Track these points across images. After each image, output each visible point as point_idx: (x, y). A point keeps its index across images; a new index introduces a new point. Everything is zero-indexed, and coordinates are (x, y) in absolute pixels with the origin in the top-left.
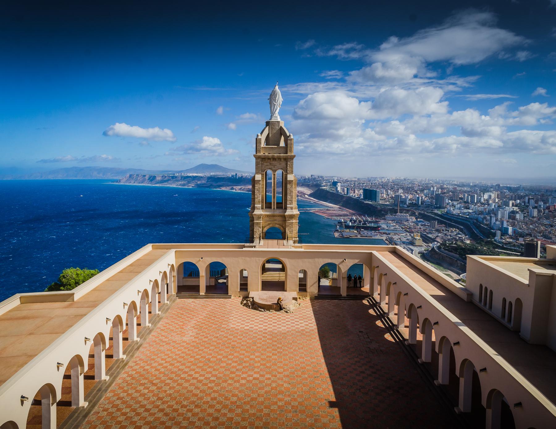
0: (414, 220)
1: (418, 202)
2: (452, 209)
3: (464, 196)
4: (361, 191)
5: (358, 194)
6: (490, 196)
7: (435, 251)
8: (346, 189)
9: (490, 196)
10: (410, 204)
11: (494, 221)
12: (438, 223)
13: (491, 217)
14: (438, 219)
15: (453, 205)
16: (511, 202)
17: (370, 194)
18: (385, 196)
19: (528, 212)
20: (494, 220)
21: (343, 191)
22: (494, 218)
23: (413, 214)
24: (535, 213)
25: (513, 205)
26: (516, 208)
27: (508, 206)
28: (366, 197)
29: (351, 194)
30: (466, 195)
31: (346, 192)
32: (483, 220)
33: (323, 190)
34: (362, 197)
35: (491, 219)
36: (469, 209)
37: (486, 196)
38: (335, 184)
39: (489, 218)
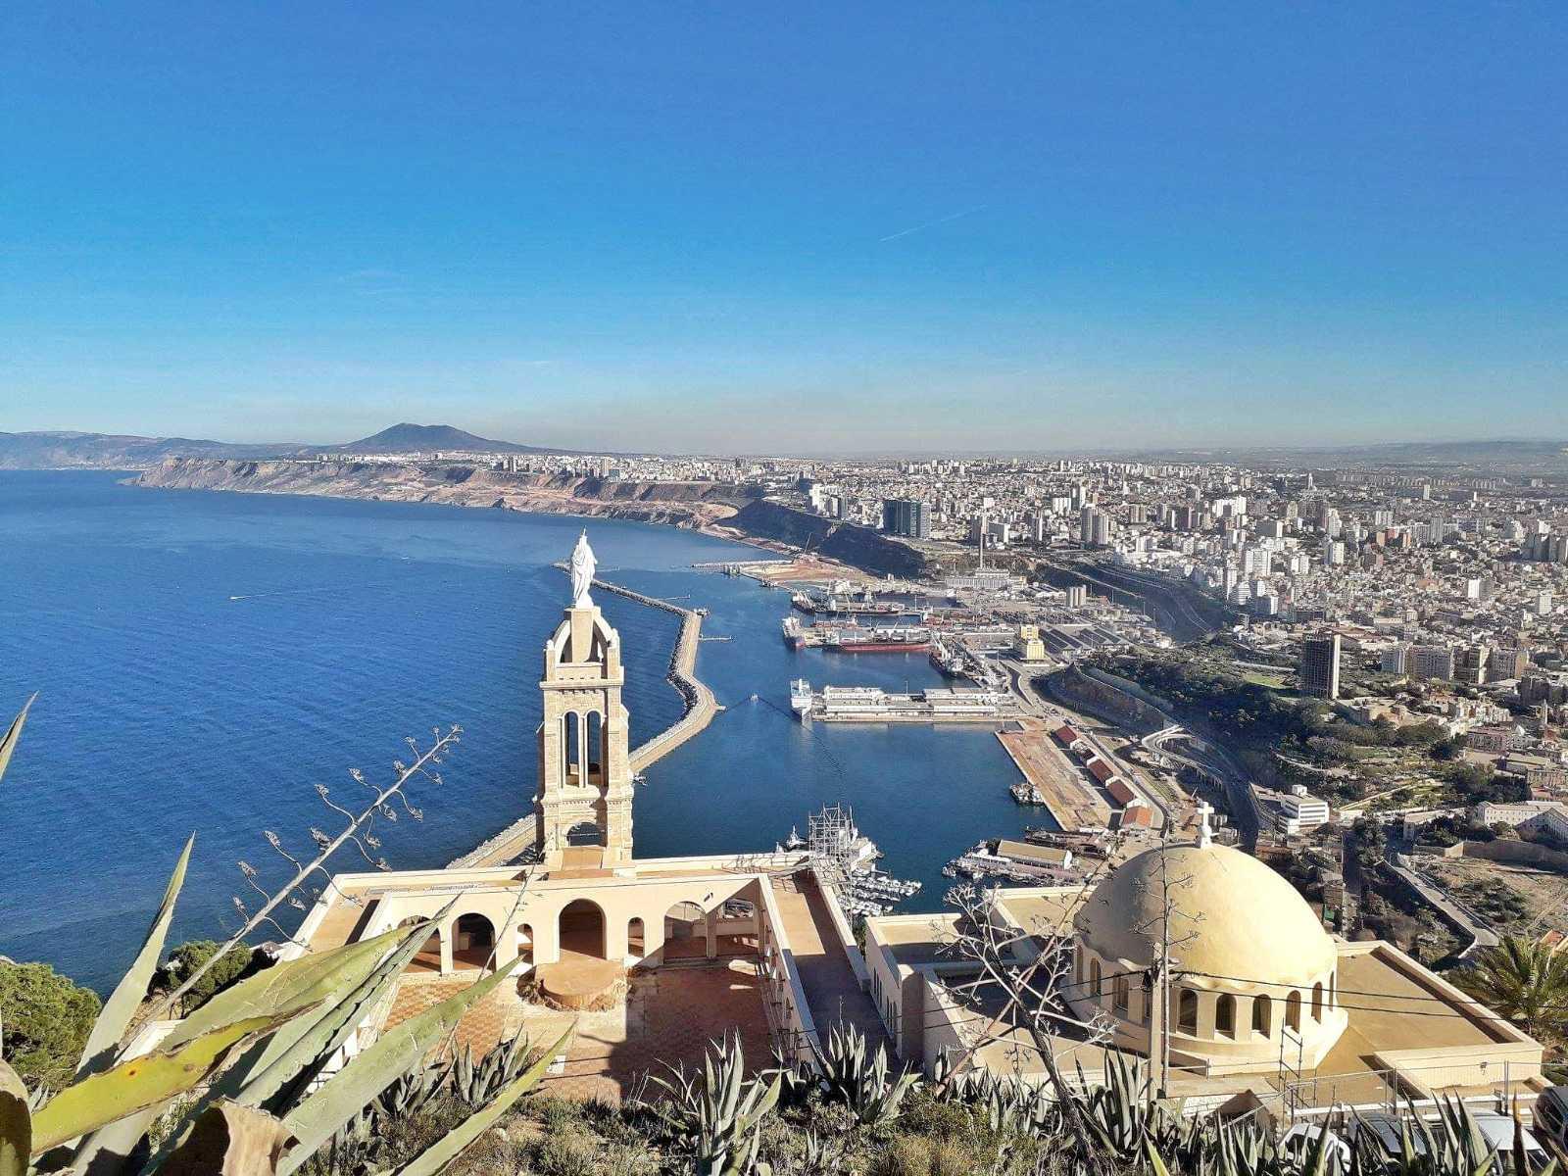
0: (1025, 586)
1: (1036, 534)
3: (1160, 509)
4: (880, 505)
5: (868, 514)
6: (1227, 509)
8: (835, 502)
9: (1227, 509)
10: (1015, 540)
12: (1088, 591)
13: (1225, 571)
14: (1087, 583)
16: (1280, 525)
18: (944, 518)
19: (1322, 552)
20: (1232, 577)
21: (829, 504)
22: (1235, 574)
23: (1021, 570)
24: (1339, 551)
25: (1285, 534)
26: (1293, 542)
27: (1273, 535)
28: (890, 527)
29: (851, 516)
30: (1165, 509)
31: (835, 509)
33: (771, 505)
34: (880, 525)
36: (1171, 548)
37: (1218, 508)
38: (804, 485)
39: (1220, 572)
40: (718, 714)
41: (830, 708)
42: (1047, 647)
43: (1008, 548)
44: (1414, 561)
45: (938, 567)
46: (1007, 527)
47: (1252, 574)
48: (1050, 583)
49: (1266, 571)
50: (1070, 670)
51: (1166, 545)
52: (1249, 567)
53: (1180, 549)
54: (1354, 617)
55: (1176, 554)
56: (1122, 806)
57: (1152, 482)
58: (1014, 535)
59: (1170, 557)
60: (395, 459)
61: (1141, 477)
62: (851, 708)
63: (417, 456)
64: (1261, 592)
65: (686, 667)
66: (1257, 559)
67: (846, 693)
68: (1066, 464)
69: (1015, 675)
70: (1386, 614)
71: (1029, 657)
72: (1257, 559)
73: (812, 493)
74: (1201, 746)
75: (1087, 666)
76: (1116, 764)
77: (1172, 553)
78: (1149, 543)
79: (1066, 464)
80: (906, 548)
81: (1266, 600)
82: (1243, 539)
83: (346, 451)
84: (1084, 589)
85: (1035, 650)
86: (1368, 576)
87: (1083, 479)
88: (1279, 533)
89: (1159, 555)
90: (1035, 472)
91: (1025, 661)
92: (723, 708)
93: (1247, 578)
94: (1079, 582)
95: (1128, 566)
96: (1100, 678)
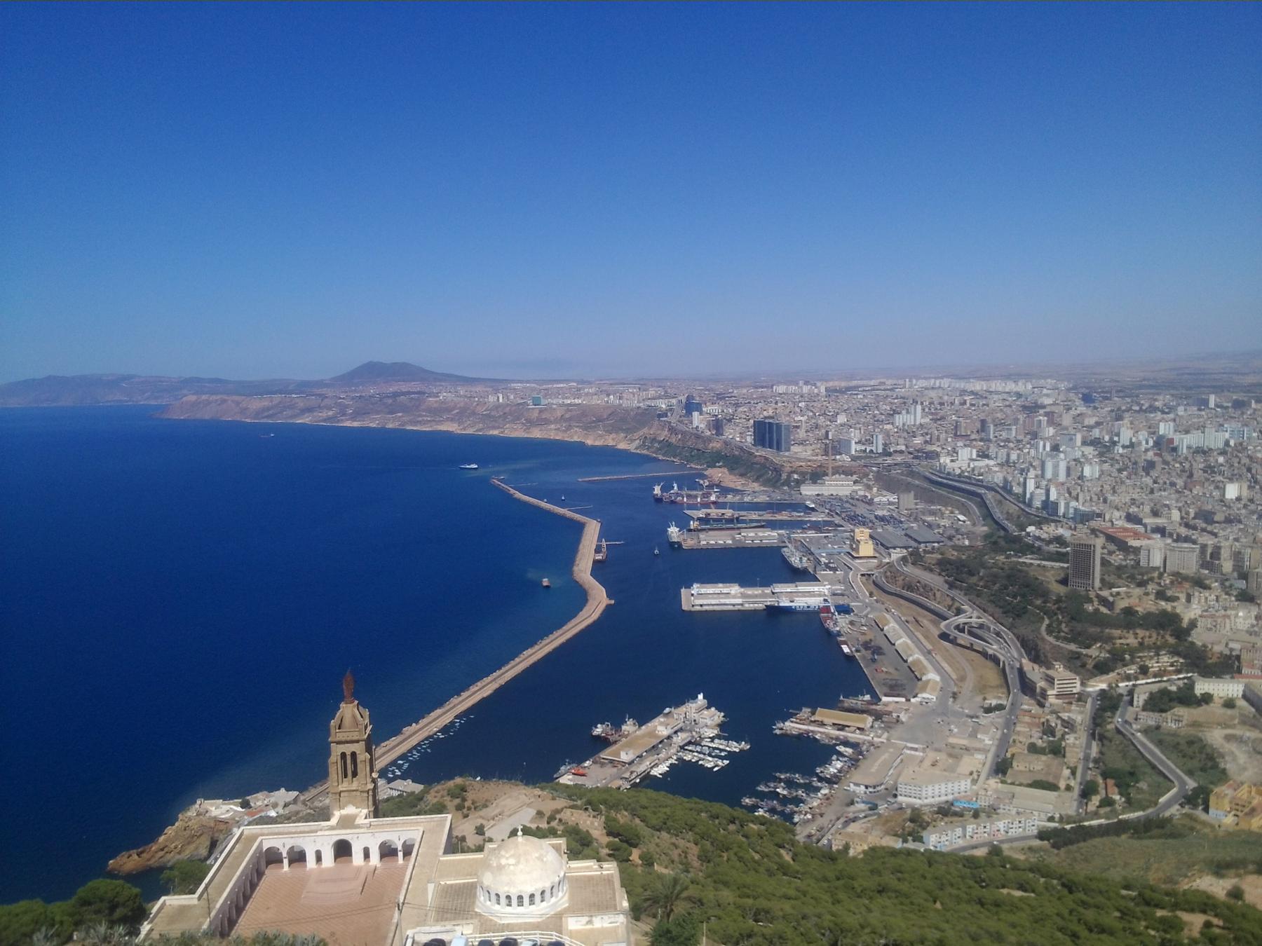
17: (767, 433)
20: (1031, 485)
35: (1025, 484)
40: (608, 606)
44: (1187, 465)
45: (796, 476)
47: (1049, 480)
49: (1062, 477)
51: (983, 455)
52: (1049, 475)
54: (1130, 518)
55: (991, 463)
58: (860, 447)
62: (713, 602)
64: (1053, 497)
66: (1056, 467)
67: (710, 589)
70: (1155, 513)
71: (861, 554)
72: (1056, 467)
77: (987, 461)
81: (1056, 504)
82: (1048, 449)
85: (867, 549)
86: (1148, 480)
88: (1079, 443)
89: (977, 463)
93: (1044, 483)
95: (949, 474)
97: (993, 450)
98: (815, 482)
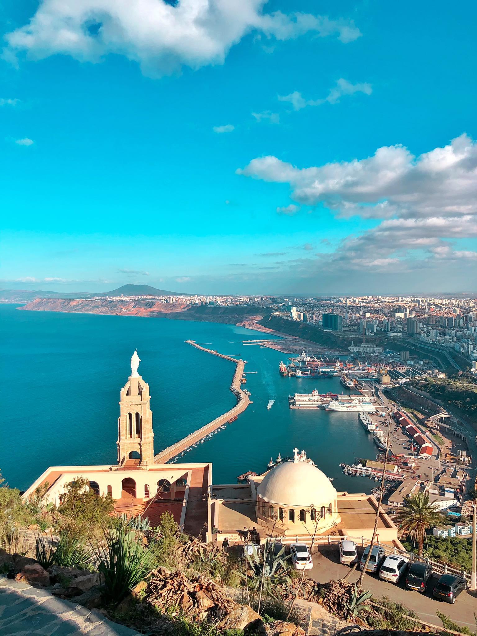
2: (426, 336)
4: (321, 315)
7: (403, 390)
8: (302, 314)
11: (472, 350)
15: (427, 331)
17: (329, 320)
21: (299, 316)
31: (302, 318)
32: (460, 348)
33: (275, 317)
34: (321, 324)
35: (468, 347)
36: (445, 335)
39: (466, 345)
41: (297, 403)
42: (391, 377)
43: (375, 334)
46: (375, 326)
48: (393, 350)
50: (400, 387)
51: (443, 334)
53: (450, 336)
55: (448, 337)
56: (420, 446)
57: (439, 307)
58: (378, 328)
59: (445, 339)
60: (125, 298)
61: (434, 304)
63: (133, 297)
65: (237, 385)
68: (402, 299)
69: (377, 390)
73: (292, 311)
74: (455, 420)
75: (407, 384)
76: (419, 428)
78: (436, 333)
79: (402, 299)
80: (332, 335)
83: (106, 296)
84: (408, 352)
87: (409, 305)
90: (389, 302)
91: (382, 384)
92: (252, 402)
94: (405, 349)
96: (412, 390)
97: (448, 331)
98: (356, 346)
